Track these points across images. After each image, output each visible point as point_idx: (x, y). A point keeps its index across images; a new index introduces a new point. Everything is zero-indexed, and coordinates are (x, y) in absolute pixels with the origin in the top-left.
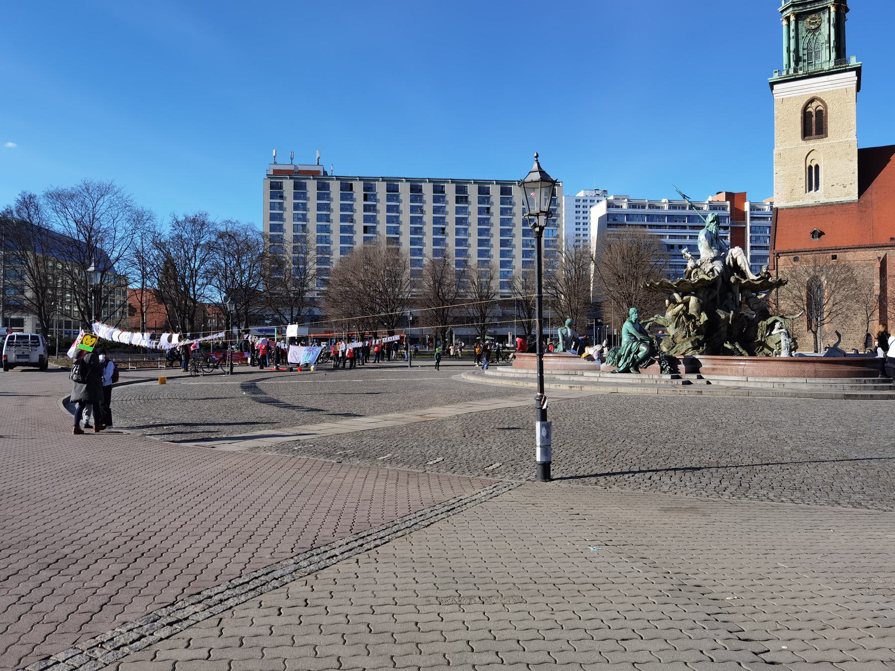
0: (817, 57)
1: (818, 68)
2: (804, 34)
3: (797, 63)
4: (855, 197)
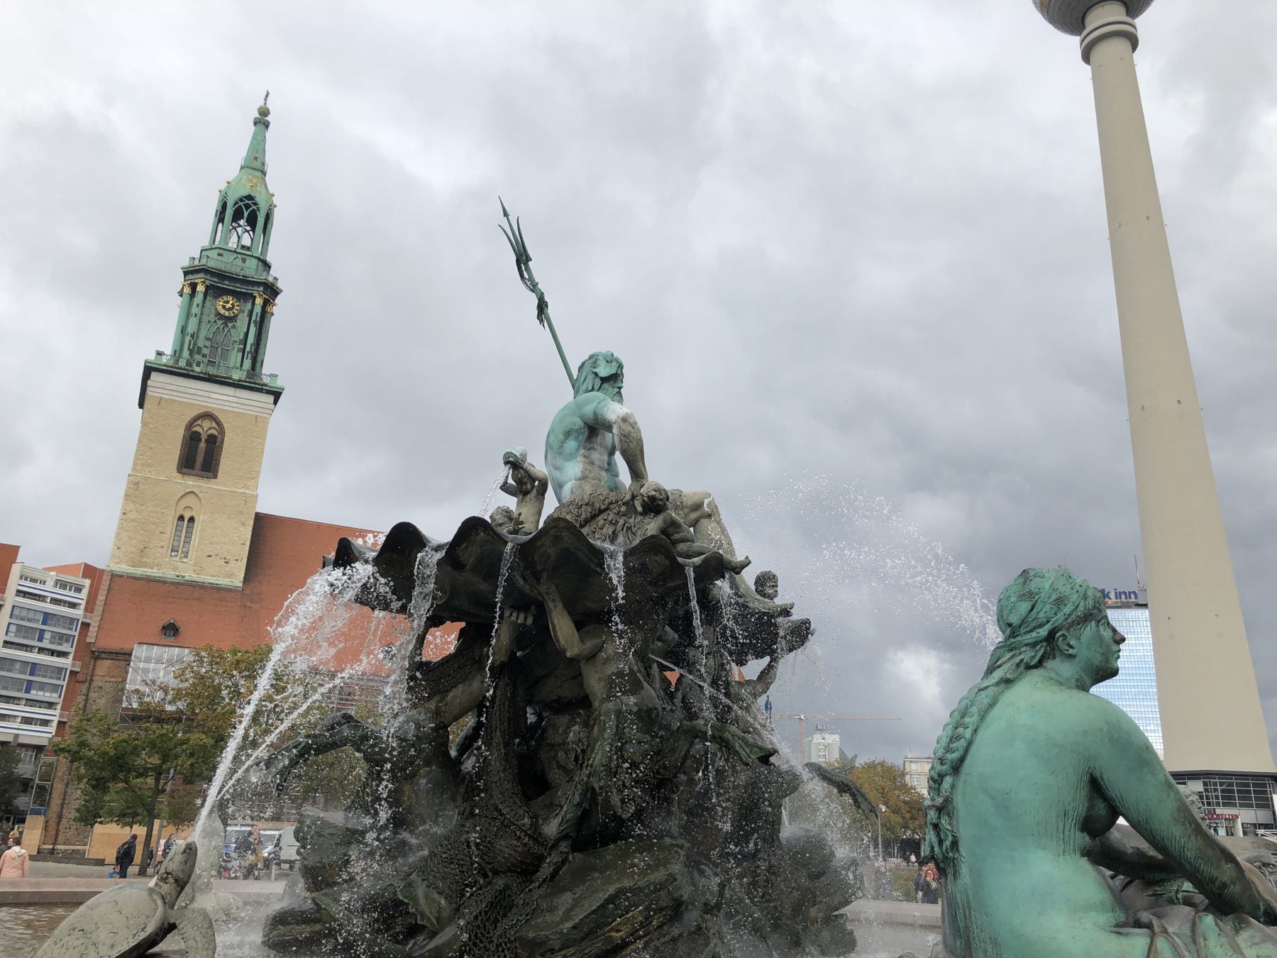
0: (225, 355)
1: (221, 372)
2: (212, 318)
3: (191, 352)
4: (238, 582)
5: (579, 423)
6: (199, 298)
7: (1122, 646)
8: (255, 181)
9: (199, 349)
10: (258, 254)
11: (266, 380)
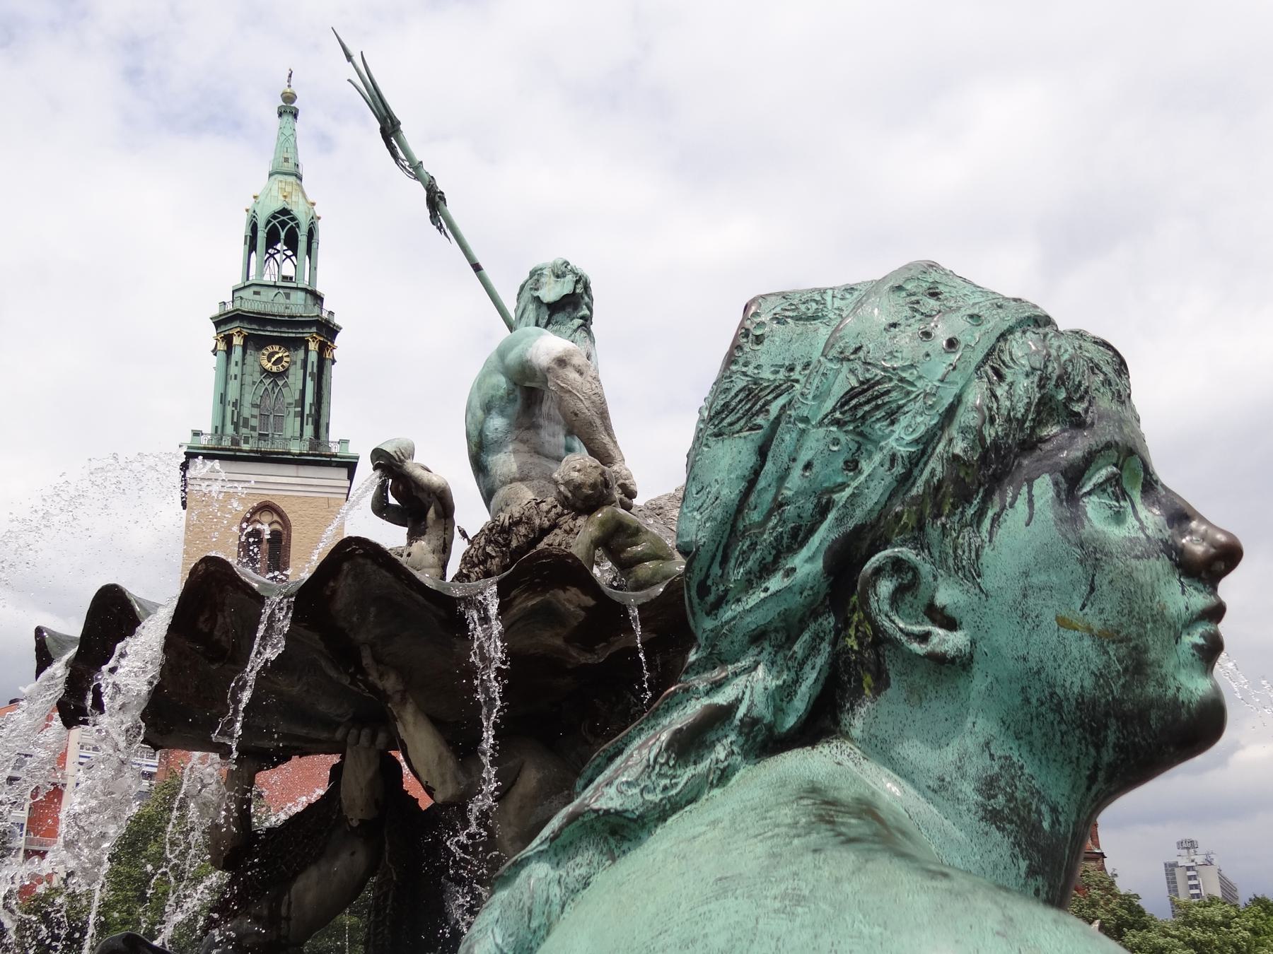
0: (279, 427)
1: (278, 447)
2: (257, 377)
3: (236, 426)
5: (501, 382)
6: (237, 354)
7: (1230, 588)
8: (288, 189)
9: (246, 421)
10: (304, 283)
11: (335, 449)
